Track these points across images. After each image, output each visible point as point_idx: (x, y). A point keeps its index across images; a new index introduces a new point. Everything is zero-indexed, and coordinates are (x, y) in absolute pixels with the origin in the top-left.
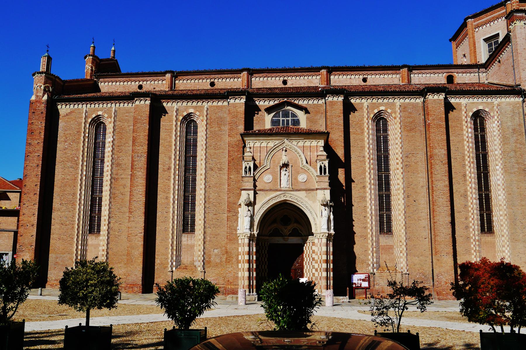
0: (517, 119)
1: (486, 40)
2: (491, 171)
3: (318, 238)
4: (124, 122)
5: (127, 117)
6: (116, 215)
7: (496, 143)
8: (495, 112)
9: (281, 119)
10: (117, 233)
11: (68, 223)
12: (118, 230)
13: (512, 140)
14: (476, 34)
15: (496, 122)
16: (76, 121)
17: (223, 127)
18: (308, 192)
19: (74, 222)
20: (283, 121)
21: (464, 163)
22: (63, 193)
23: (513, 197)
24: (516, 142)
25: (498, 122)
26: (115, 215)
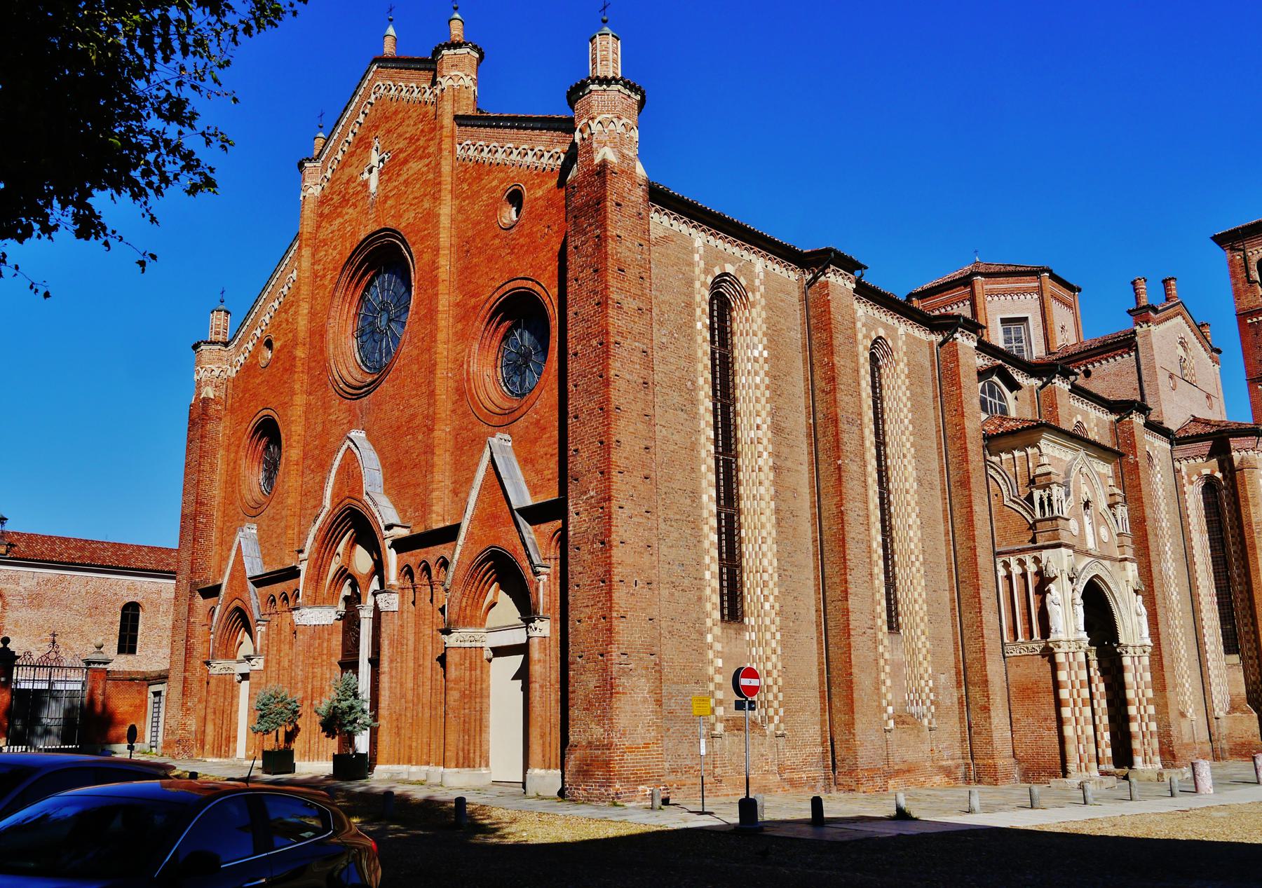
3: (1133, 654)
4: (779, 313)
5: (783, 304)
6: (786, 573)
7: (1162, 508)
9: (989, 399)
10: (791, 624)
11: (686, 582)
12: (794, 616)
13: (1171, 506)
15: (1159, 476)
16: (680, 271)
17: (925, 389)
18: (1113, 562)
19: (702, 582)
20: (991, 402)
22: (668, 484)
25: (1162, 476)
26: (784, 570)
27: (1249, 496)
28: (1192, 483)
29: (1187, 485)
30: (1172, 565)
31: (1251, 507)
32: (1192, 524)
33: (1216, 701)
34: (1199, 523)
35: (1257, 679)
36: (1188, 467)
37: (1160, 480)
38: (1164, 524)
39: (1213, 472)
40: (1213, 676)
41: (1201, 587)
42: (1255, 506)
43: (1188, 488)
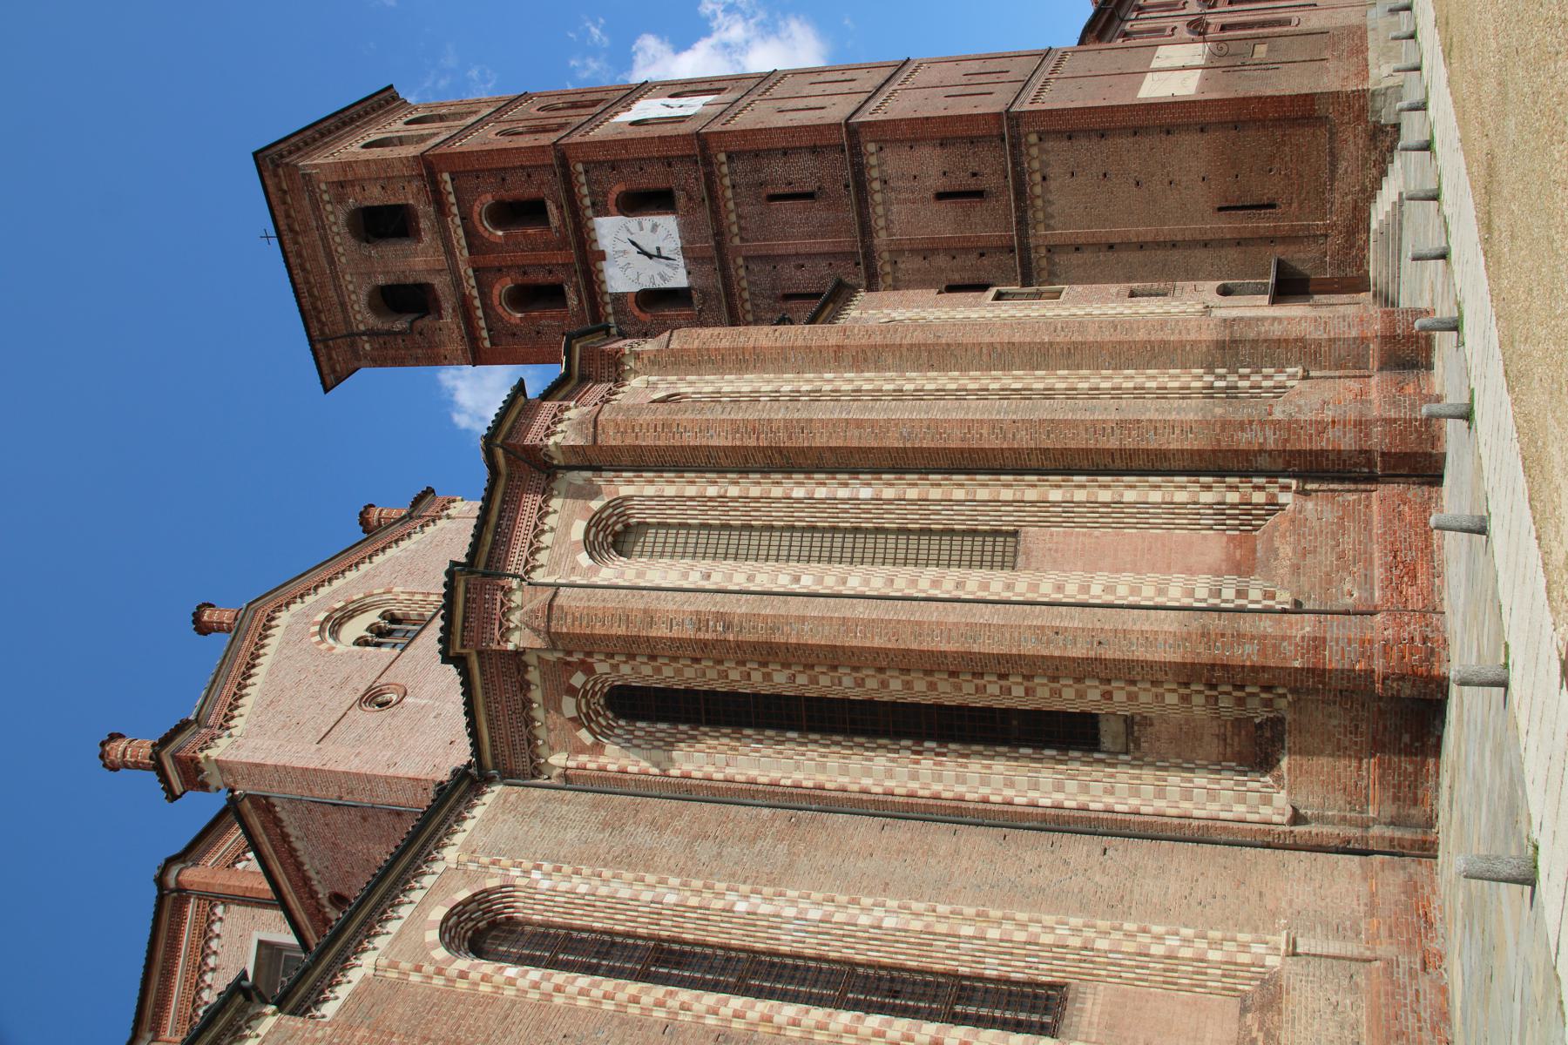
0: (565, 808)
2: (748, 942)
7: (625, 893)
8: (493, 869)
15: (536, 875)
21: (658, 1029)
23: (906, 878)
24: (661, 829)
25: (538, 867)
27: (622, 631)
28: (597, 749)
29: (602, 760)
30: (793, 902)
31: (653, 633)
32: (709, 769)
33: (1240, 810)
35: (1174, 691)
37: (548, 875)
38: (671, 898)
39: (572, 691)
40: (1160, 805)
41: (889, 784)
42: (651, 623)
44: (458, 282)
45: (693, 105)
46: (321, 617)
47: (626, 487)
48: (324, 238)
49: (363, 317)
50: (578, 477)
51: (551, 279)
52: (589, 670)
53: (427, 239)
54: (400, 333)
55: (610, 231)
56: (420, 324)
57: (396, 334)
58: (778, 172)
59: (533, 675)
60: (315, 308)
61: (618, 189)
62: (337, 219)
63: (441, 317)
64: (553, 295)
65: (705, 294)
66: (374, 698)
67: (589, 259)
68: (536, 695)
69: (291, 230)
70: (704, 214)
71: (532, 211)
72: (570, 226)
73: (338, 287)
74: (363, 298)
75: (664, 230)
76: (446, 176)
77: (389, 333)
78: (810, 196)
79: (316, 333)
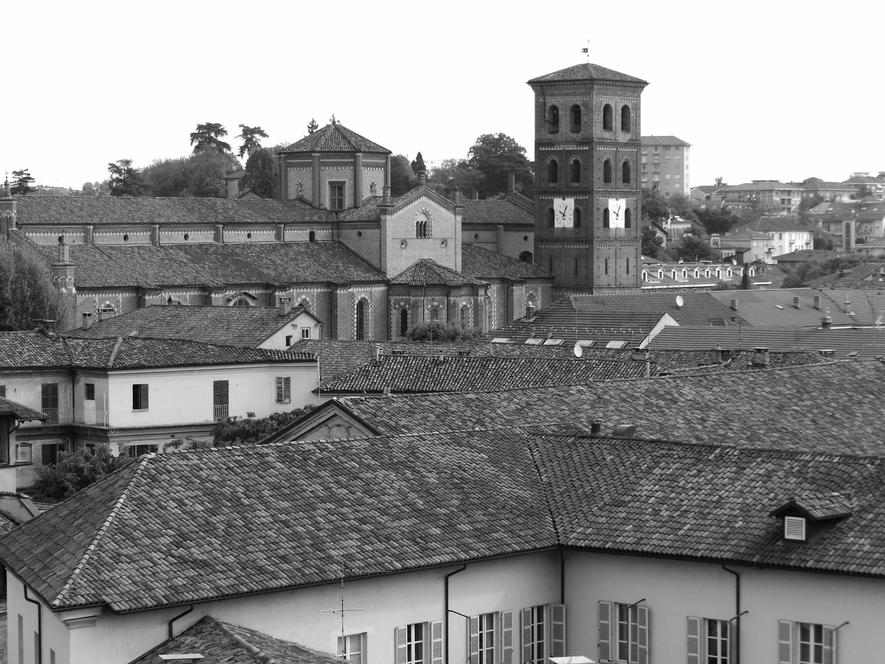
1: (330, 182)
14: (321, 172)
34: (396, 331)
36: (395, 299)
39: (405, 305)
43: (394, 312)
44: (559, 143)
45: (617, 222)
46: (424, 209)
47: (444, 312)
48: (571, 94)
49: (551, 101)
50: (446, 301)
51: (558, 179)
52: (409, 308)
53: (571, 134)
54: (545, 115)
55: (570, 202)
56: (547, 124)
57: (544, 113)
58: (582, 264)
59: (407, 297)
60: (551, 86)
61: (581, 209)
62: (578, 100)
63: (550, 133)
64: (554, 178)
65: (553, 232)
66: (404, 242)
67: (564, 194)
68: (404, 297)
69: (574, 85)
70: (573, 235)
71: (577, 179)
72: (572, 190)
73: (559, 95)
74: (555, 104)
75: (569, 223)
76: (587, 148)
77: (545, 111)
78: (576, 273)
79: (543, 84)
